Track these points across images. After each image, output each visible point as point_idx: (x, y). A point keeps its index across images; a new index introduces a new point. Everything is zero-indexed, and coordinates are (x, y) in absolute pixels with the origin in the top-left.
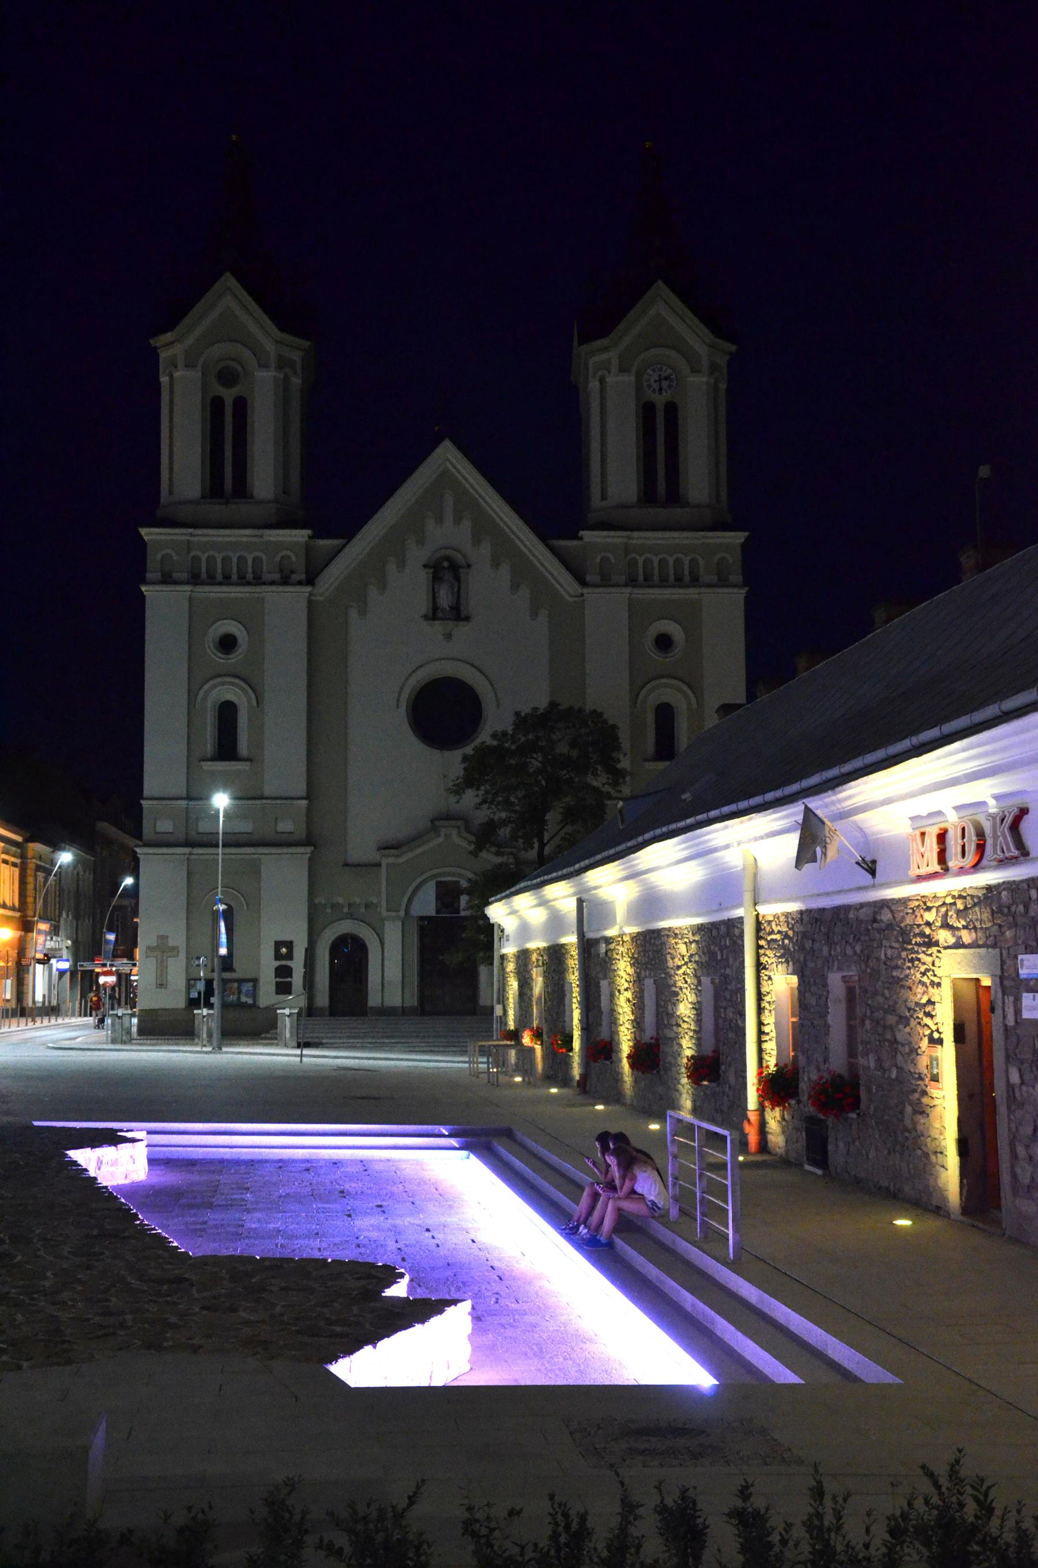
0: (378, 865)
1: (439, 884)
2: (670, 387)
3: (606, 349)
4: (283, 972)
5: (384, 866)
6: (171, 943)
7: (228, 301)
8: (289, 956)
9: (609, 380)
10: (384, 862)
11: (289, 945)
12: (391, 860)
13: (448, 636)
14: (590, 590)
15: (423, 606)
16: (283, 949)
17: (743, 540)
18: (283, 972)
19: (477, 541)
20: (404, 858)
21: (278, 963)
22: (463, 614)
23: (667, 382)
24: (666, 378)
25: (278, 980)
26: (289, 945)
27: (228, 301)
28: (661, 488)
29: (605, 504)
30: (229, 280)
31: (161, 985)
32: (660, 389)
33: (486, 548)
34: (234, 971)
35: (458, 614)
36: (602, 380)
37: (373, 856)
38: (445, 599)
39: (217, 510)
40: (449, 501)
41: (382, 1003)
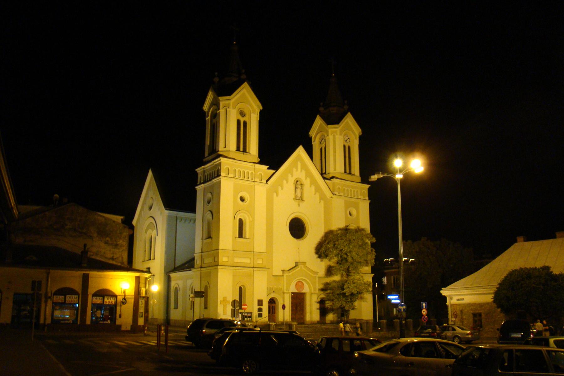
0: (283, 276)
3: (337, 128)
4: (260, 310)
5: (285, 276)
8: (262, 305)
9: (337, 137)
12: (287, 274)
13: (299, 205)
14: (335, 196)
15: (293, 196)
16: (260, 302)
17: (368, 187)
18: (260, 310)
19: (306, 179)
20: (290, 274)
22: (303, 200)
25: (259, 312)
27: (244, 90)
28: (348, 171)
29: (335, 171)
30: (246, 84)
33: (308, 180)
35: (302, 199)
36: (334, 136)
37: (281, 274)
38: (299, 194)
39: (240, 155)
40: (299, 165)
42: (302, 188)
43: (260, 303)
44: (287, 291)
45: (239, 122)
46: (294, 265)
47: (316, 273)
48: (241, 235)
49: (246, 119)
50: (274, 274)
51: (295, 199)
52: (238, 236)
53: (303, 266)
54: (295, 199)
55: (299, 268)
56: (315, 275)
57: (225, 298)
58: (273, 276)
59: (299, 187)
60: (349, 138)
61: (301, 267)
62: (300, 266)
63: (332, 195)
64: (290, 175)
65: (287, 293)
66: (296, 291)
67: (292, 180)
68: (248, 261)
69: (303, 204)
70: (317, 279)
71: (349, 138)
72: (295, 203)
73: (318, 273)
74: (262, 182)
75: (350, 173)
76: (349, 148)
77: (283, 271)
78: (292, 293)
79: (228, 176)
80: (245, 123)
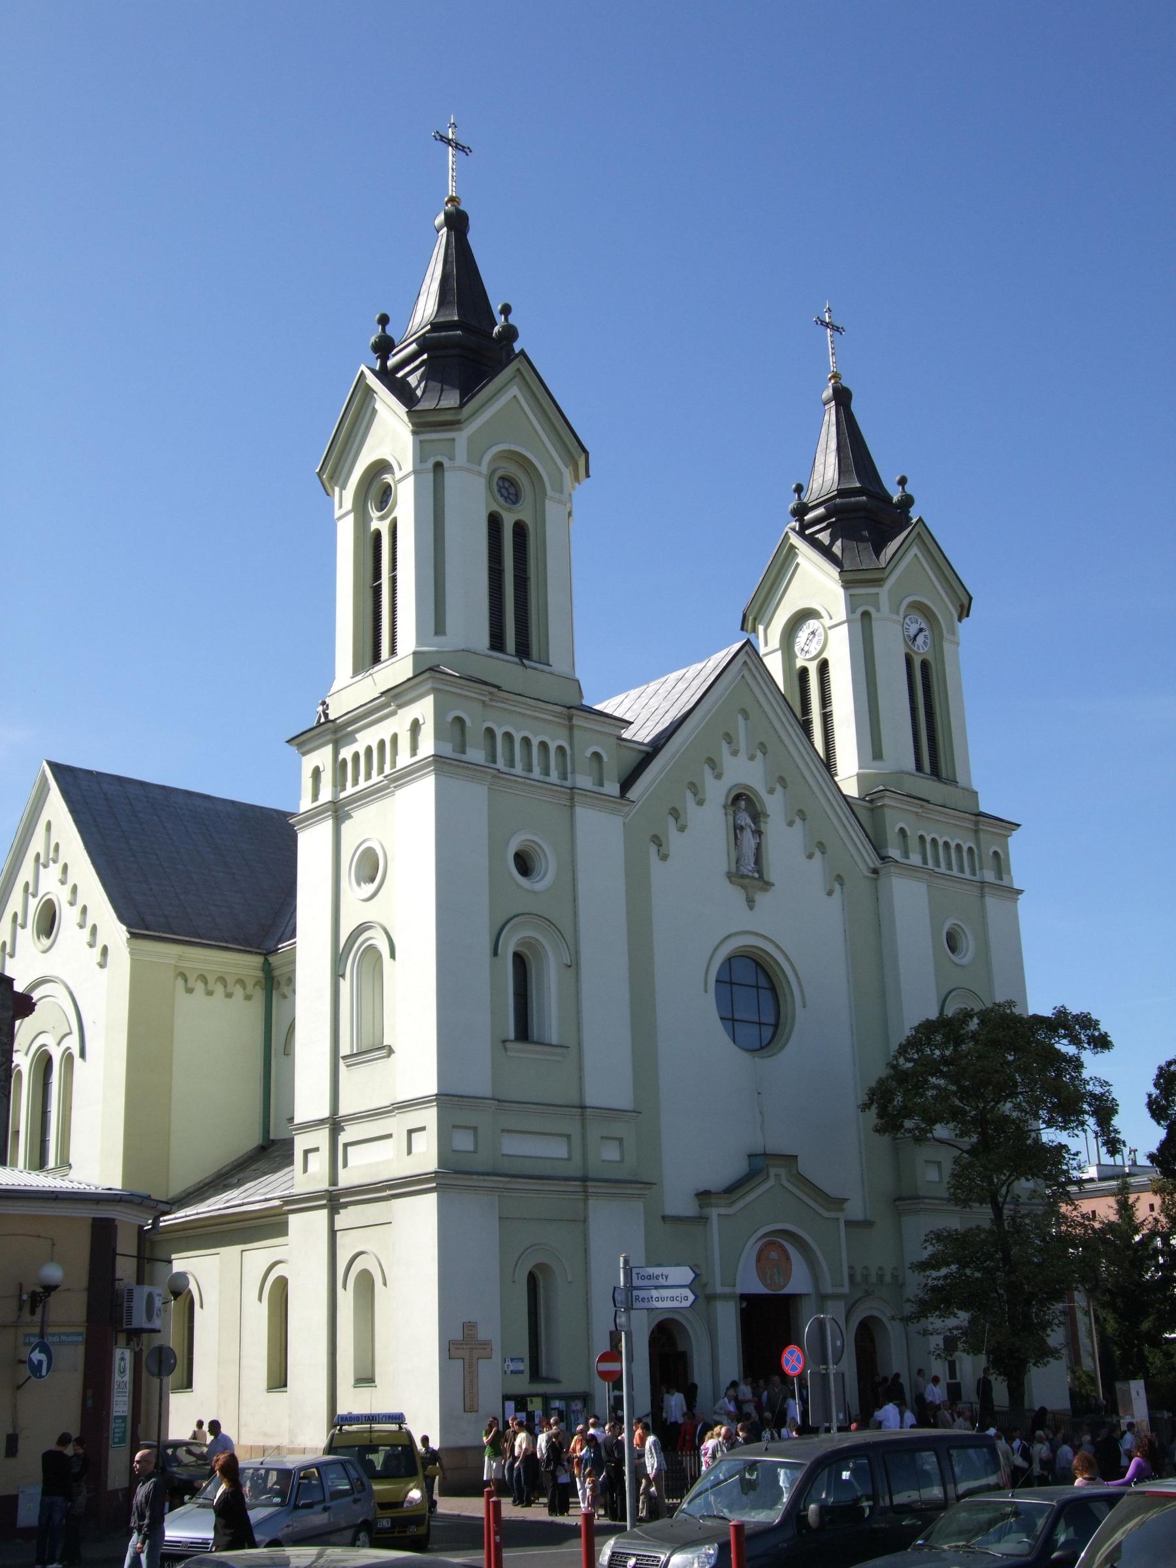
0: (702, 1220)
5: (714, 1219)
6: (482, 1335)
7: (514, 390)
10: (714, 1213)
12: (723, 1211)
13: (751, 903)
22: (765, 878)
27: (514, 390)
34: (557, 1381)
42: (758, 833)
44: (727, 1290)
45: (494, 522)
46: (736, 1168)
47: (839, 1203)
48: (523, 1032)
49: (524, 513)
50: (670, 1210)
52: (512, 1036)
53: (782, 1172)
54: (735, 876)
55: (771, 1182)
56: (833, 1215)
58: (664, 1218)
59: (745, 819)
60: (921, 630)
61: (777, 1176)
62: (772, 1171)
63: (878, 863)
65: (726, 1297)
66: (758, 1288)
67: (717, 792)
68: (558, 1149)
69: (761, 898)
70: (842, 1225)
71: (921, 630)
72: (736, 895)
73: (845, 1205)
74: (605, 790)
75: (935, 772)
76: (925, 665)
77: (704, 1196)
78: (743, 1297)
79: (464, 757)
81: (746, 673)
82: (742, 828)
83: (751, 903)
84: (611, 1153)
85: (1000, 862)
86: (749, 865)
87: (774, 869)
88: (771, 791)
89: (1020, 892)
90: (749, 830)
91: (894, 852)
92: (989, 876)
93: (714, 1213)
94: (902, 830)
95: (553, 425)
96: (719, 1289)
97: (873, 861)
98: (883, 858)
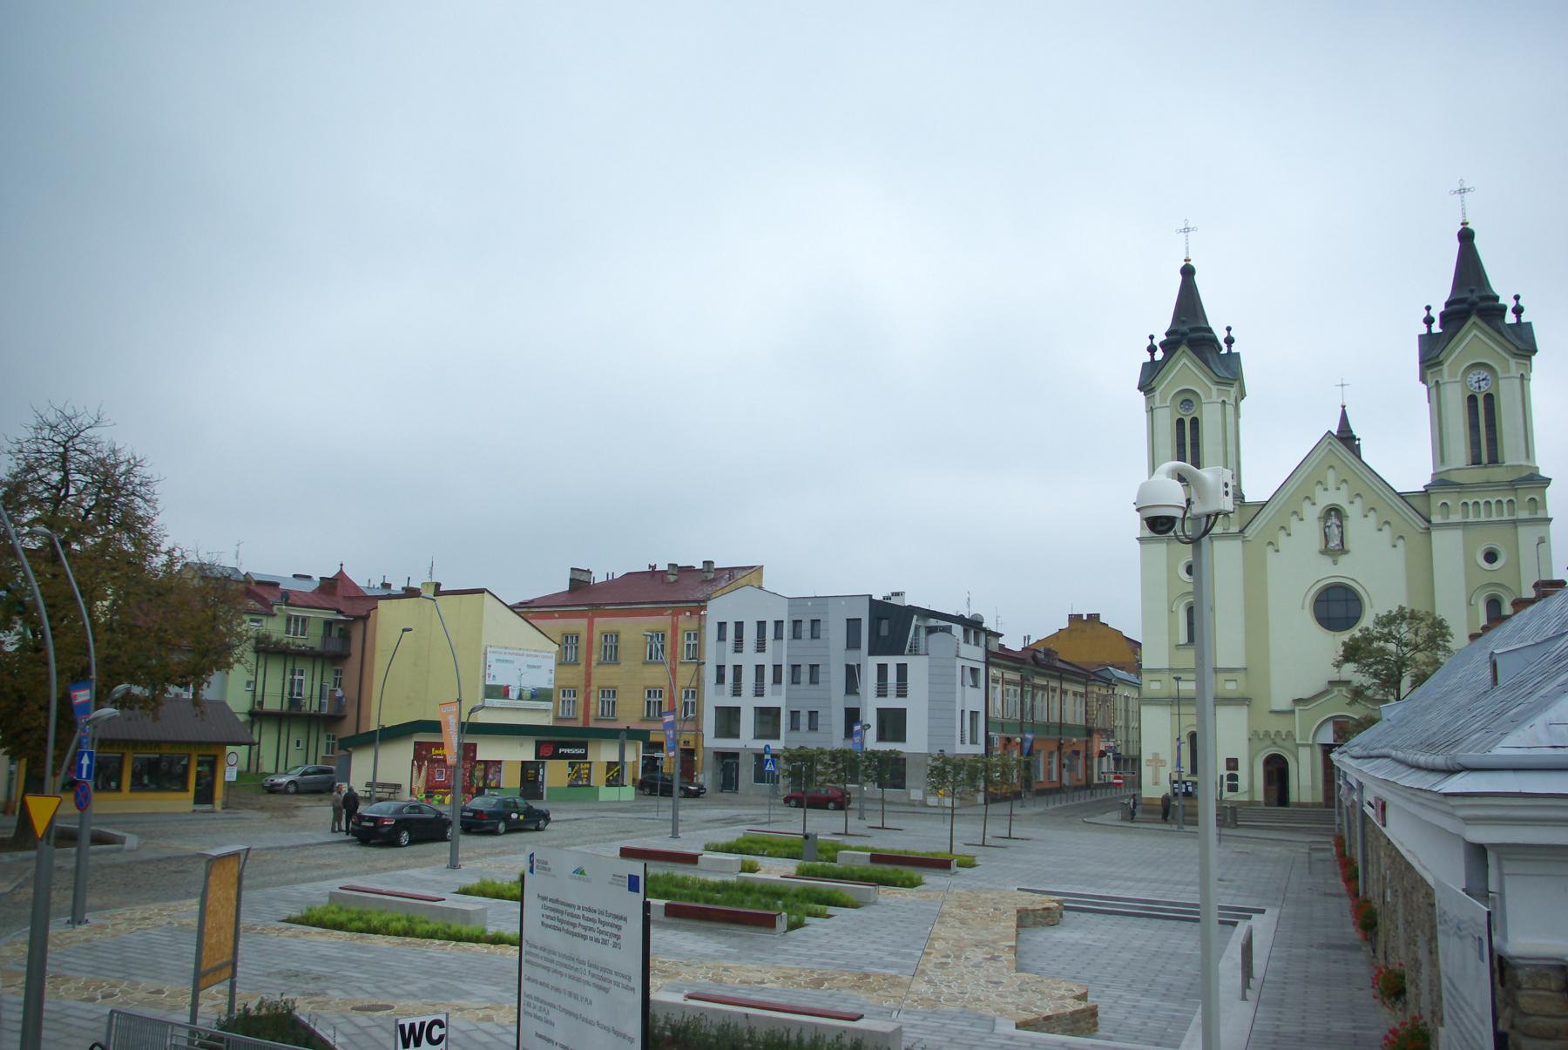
0: (1293, 712)
1: (1336, 724)
2: (1486, 384)
6: (1161, 757)
7: (1184, 360)
8: (1236, 768)
10: (1297, 709)
11: (1235, 761)
12: (1301, 708)
13: (1335, 563)
15: (1317, 541)
21: (1228, 772)
23: (1484, 382)
24: (1483, 380)
26: (1235, 761)
27: (1184, 360)
31: (1156, 783)
32: (1480, 387)
35: (1342, 549)
41: (1299, 799)
42: (1340, 526)
43: (1232, 764)
45: (1180, 422)
51: (1326, 551)
53: (1344, 689)
54: (1326, 551)
55: (1336, 693)
57: (1156, 755)
58: (1272, 712)
59: (1334, 520)
63: (1427, 525)
64: (1307, 504)
67: (1312, 513)
69: (1343, 559)
72: (1327, 560)
74: (1231, 531)
76: (1489, 398)
77: (1298, 701)
80: (1195, 422)
81: (1330, 447)
82: (1329, 527)
83: (1335, 563)
84: (1231, 686)
85: (1537, 504)
86: (1334, 543)
87: (1350, 544)
88: (1352, 503)
89: (1550, 520)
90: (1334, 526)
91: (1436, 519)
92: (1523, 514)
93: (1297, 709)
94: (1445, 504)
95: (1201, 367)
96: (1298, 742)
97: (1423, 524)
98: (1429, 521)
